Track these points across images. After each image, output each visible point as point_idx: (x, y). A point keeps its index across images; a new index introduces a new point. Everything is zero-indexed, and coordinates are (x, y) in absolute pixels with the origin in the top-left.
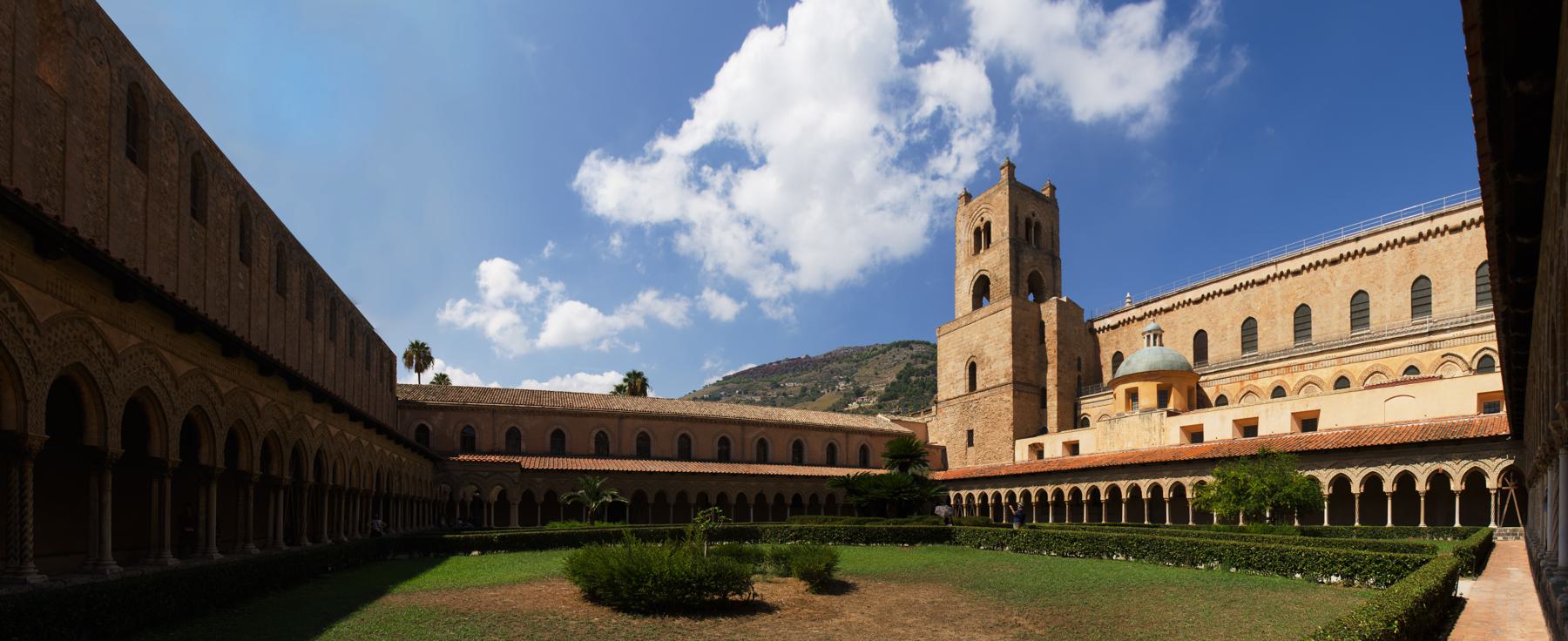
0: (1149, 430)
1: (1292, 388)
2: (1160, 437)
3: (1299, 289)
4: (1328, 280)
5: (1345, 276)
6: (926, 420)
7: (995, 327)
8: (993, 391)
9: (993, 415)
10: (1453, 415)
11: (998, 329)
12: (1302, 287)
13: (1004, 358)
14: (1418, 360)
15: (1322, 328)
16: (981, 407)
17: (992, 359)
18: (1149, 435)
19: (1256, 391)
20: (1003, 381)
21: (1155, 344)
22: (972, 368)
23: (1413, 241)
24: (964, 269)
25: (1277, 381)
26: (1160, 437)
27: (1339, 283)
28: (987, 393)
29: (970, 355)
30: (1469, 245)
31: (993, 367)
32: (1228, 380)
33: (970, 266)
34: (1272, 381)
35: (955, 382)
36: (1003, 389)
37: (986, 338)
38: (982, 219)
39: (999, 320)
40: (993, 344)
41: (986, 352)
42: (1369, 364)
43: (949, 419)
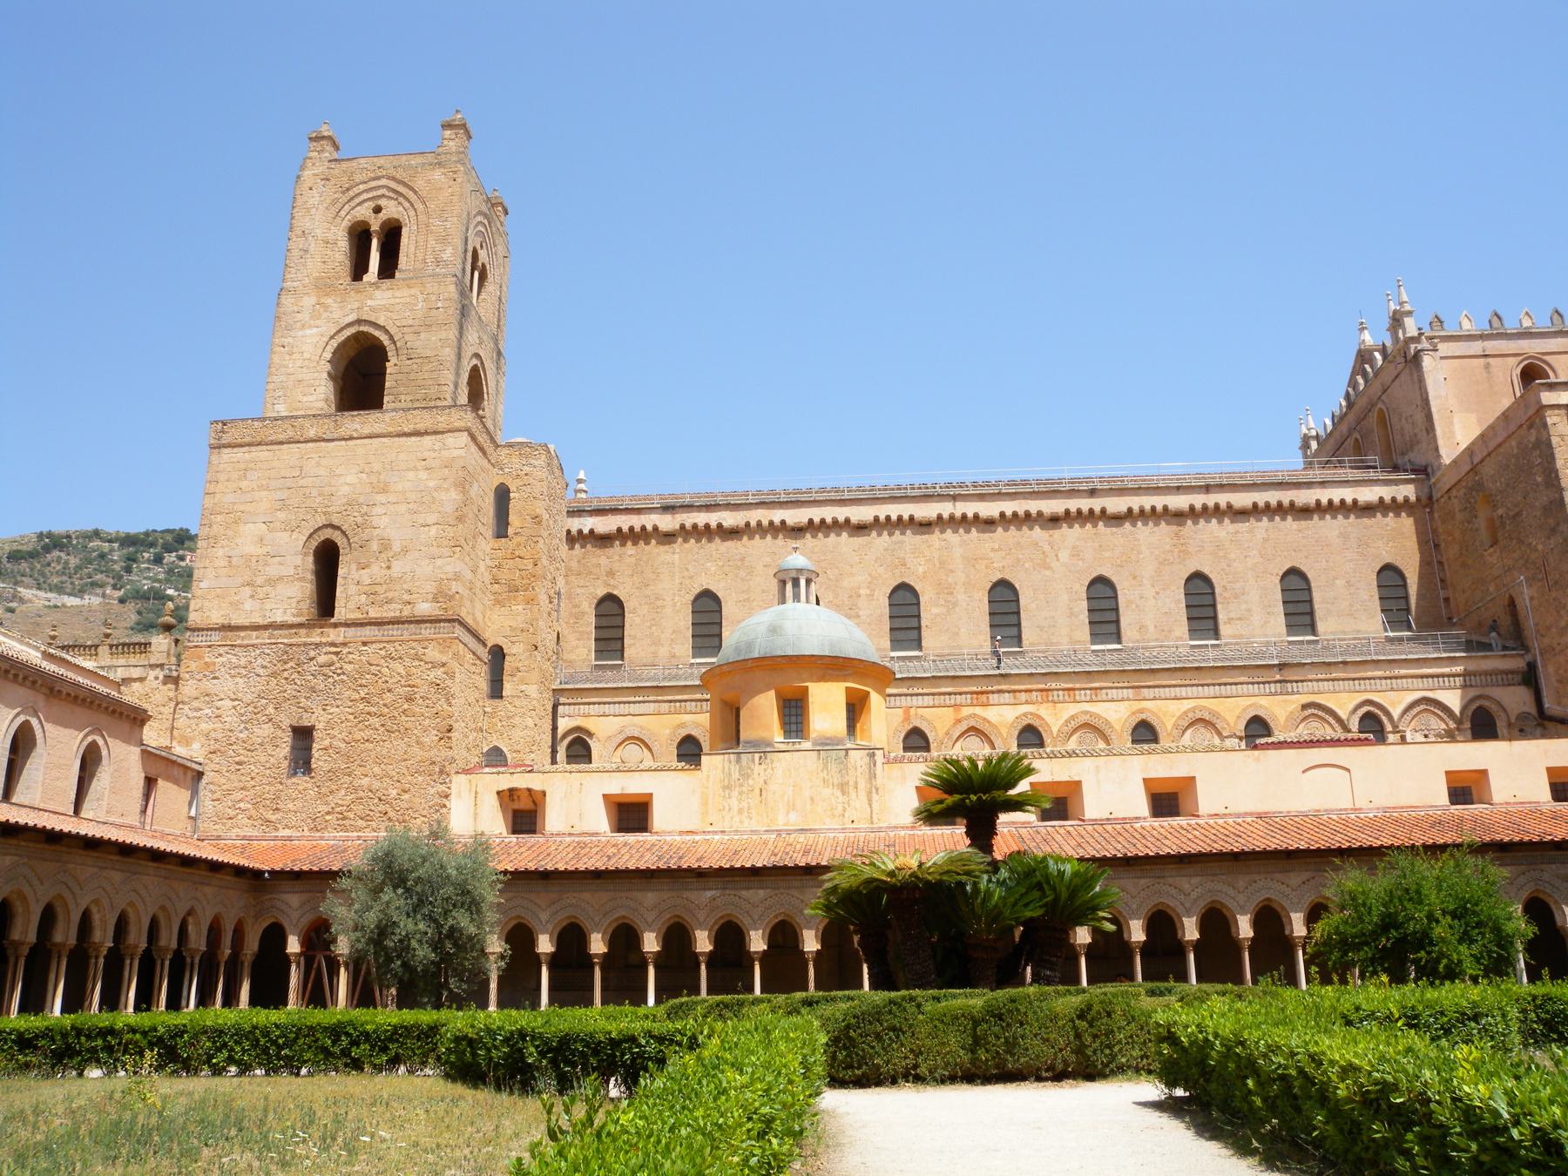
0: (843, 787)
1: (1055, 730)
2: (870, 805)
3: (993, 550)
4: (1046, 548)
5: (1074, 547)
6: (119, 674)
7: (415, 469)
8: (394, 631)
9: (388, 697)
10: (1248, 811)
11: (423, 475)
12: (1000, 549)
13: (435, 551)
14: (1266, 709)
15: (1041, 628)
16: (348, 667)
17: (396, 547)
18: (841, 799)
19: (986, 729)
20: (425, 608)
21: (807, 601)
22: (327, 559)
23: (1178, 517)
24: (309, 301)
25: (1025, 715)
26: (870, 805)
27: (1064, 555)
28: (368, 632)
29: (321, 521)
30: (1266, 540)
31: (398, 568)
32: (928, 700)
33: (329, 301)
34: (1018, 714)
35: (259, 581)
36: (426, 631)
37: (384, 491)
38: (377, 210)
39: (426, 454)
40: (403, 508)
41: (376, 521)
42: (1187, 705)
43: (226, 685)
